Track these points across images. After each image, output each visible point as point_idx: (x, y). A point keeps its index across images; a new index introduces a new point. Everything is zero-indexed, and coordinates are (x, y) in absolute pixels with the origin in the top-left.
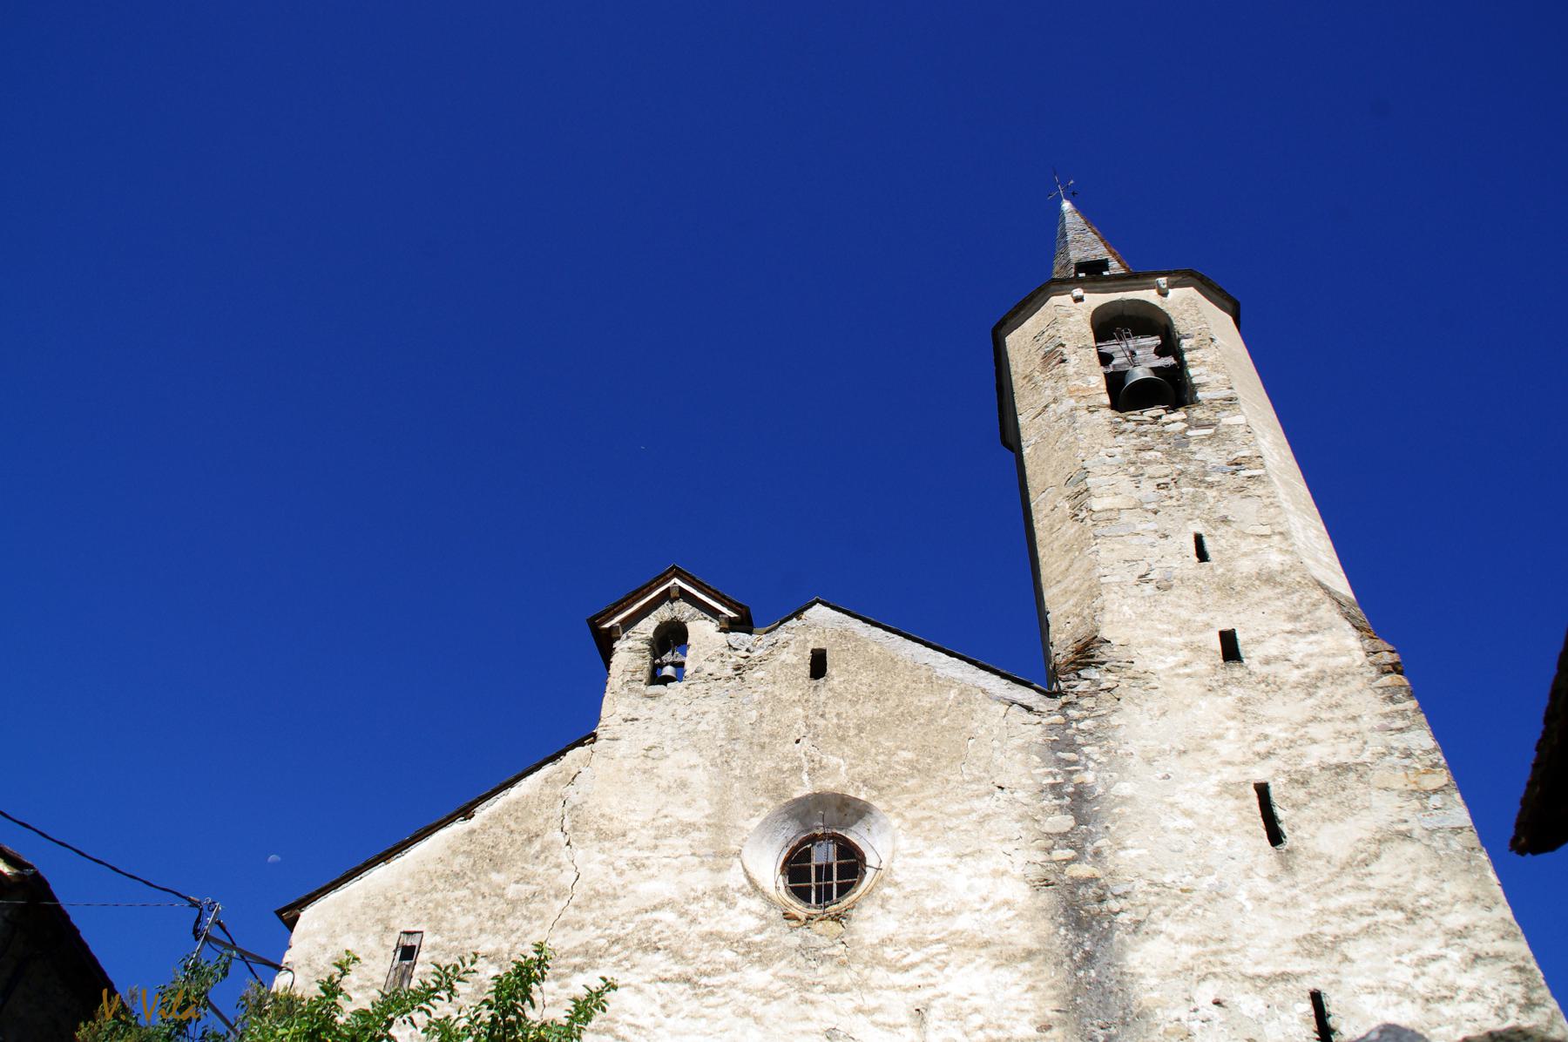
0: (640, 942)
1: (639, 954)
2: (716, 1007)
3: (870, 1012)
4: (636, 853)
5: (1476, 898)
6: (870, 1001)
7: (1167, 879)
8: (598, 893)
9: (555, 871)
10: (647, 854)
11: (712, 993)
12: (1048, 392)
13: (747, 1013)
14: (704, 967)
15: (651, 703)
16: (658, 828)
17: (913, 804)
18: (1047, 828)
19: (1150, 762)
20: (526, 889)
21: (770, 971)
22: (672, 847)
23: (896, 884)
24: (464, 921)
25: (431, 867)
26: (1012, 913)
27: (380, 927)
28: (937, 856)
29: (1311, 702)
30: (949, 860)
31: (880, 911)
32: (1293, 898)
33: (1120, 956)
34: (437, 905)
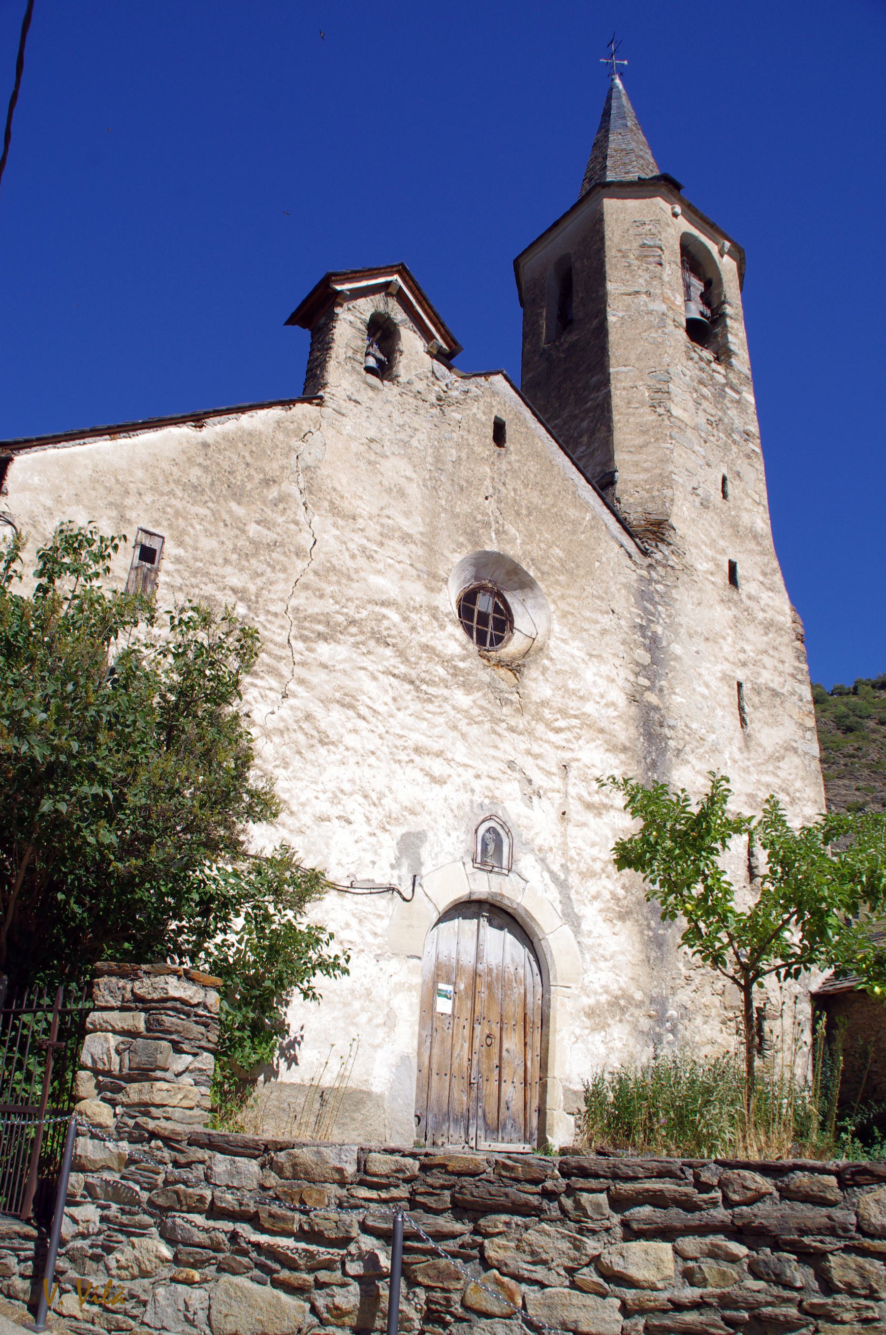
0: (373, 633)
1: (372, 643)
2: (434, 714)
3: (537, 757)
4: (365, 541)
5: (816, 802)
6: (536, 749)
7: (694, 726)
8: (334, 568)
9: (292, 526)
10: (375, 547)
11: (431, 701)
12: (641, 281)
13: (455, 728)
14: (423, 675)
15: (371, 393)
16: (382, 525)
17: (563, 597)
18: (636, 657)
19: (691, 636)
20: (270, 536)
21: (471, 697)
22: (395, 551)
23: (551, 659)
24: (208, 544)
25: (165, 465)
26: (616, 714)
27: (114, 513)
28: (575, 648)
29: (765, 639)
30: (582, 654)
31: (541, 677)
32: (748, 767)
33: (669, 770)
34: (177, 514)
